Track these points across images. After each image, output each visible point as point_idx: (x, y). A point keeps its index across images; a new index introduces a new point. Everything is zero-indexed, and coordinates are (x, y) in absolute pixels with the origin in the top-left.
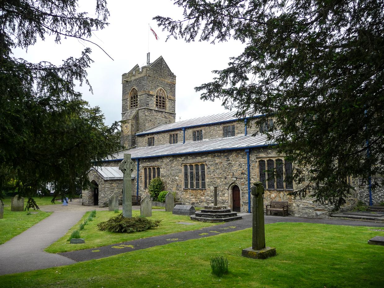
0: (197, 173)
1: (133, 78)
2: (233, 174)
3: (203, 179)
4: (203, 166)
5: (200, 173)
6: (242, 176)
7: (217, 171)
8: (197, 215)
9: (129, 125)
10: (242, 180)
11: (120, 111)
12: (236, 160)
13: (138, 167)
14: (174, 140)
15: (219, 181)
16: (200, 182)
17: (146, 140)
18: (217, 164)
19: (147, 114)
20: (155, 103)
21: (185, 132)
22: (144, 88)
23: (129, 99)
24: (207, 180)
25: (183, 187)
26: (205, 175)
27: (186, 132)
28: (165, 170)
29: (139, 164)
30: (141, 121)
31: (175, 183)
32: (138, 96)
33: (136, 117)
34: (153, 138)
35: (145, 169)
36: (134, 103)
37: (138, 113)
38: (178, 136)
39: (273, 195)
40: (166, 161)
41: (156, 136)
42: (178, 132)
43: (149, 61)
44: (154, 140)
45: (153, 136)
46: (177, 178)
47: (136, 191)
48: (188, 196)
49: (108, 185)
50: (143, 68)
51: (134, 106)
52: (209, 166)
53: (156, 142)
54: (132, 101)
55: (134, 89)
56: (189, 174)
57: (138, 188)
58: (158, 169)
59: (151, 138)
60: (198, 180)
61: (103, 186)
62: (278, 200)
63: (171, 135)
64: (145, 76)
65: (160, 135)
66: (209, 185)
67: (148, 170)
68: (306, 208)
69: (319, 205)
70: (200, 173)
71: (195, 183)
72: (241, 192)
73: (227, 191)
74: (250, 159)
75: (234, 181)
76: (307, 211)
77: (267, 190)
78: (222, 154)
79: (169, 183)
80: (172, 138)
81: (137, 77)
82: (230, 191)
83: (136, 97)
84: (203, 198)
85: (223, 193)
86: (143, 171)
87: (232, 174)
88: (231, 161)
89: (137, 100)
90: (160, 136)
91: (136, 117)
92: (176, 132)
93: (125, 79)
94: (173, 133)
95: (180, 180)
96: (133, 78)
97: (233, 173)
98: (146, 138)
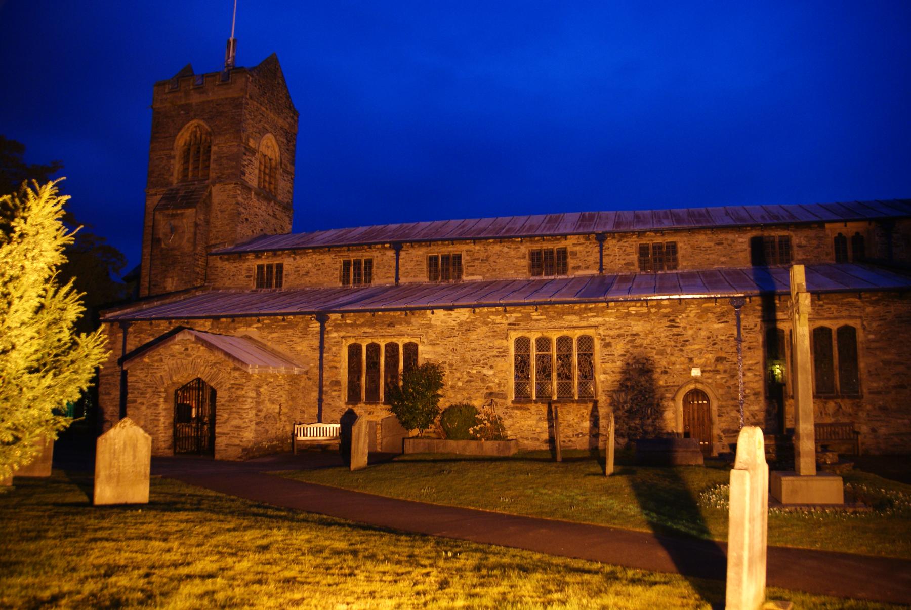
0: (565, 358)
4: (586, 341)
6: (720, 367)
10: (718, 377)
12: (699, 326)
18: (637, 334)
20: (257, 171)
21: (398, 255)
27: (403, 254)
38: (375, 263)
46: (491, 372)
59: (270, 267)
74: (743, 324)
78: (653, 310)
88: (685, 328)
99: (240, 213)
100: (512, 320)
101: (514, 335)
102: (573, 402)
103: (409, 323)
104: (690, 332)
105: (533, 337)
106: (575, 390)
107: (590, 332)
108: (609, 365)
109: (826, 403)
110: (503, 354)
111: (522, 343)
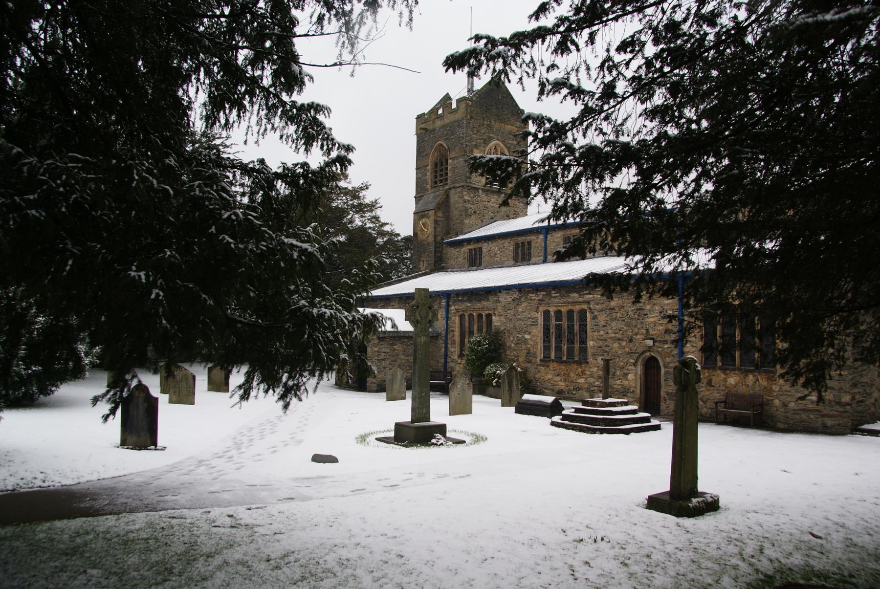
0: (571, 327)
1: (439, 123)
2: (647, 330)
3: (583, 341)
4: (583, 313)
5: (576, 328)
6: (667, 337)
7: (614, 324)
8: (566, 417)
9: (430, 222)
10: (666, 346)
11: (413, 192)
13: (448, 311)
14: (523, 254)
15: (616, 345)
16: (577, 346)
17: (464, 253)
18: (613, 309)
19: (466, 198)
21: (546, 237)
22: (462, 144)
23: (429, 167)
24: (590, 343)
25: (540, 356)
26: (586, 332)
27: (549, 236)
28: (503, 319)
29: (448, 306)
30: (455, 213)
31: (524, 346)
32: (450, 161)
33: (444, 205)
34: (481, 249)
35: (462, 317)
36: (441, 175)
37: (448, 196)
38: (533, 245)
39: (732, 380)
40: (505, 298)
41: (486, 244)
42: (532, 237)
43: (472, 87)
44: (481, 254)
45: (479, 245)
46: (527, 337)
47: (443, 361)
48: (550, 376)
49: (385, 348)
50: (459, 101)
51: (441, 181)
52: (596, 313)
53: (485, 259)
54: (436, 172)
55: (441, 145)
56: (553, 330)
57: (446, 355)
58: (489, 316)
59: (475, 249)
60: (571, 341)
61: (376, 349)
62: (742, 389)
63: (517, 245)
64: (463, 119)
65: (495, 244)
66: (594, 355)
67: (467, 318)
68: (801, 410)
69: (832, 406)
70: (576, 328)
71: (565, 348)
72: (663, 371)
73: (633, 368)
75: (650, 347)
76: (804, 416)
77: (720, 369)
79: (510, 347)
80: (520, 250)
81: (446, 121)
82: (639, 369)
83: (444, 163)
84: (582, 380)
85: (625, 371)
86: (457, 319)
87: (644, 331)
89: (447, 169)
90: (494, 246)
91: (444, 205)
92: (529, 238)
93: (423, 126)
94: (521, 239)
95: (535, 341)
96: (439, 123)
97: (647, 330)
98: (466, 249)
99: (466, 210)
100: (540, 297)
101: (542, 309)
102: (574, 362)
103: (488, 300)
104: (648, 307)
105: (552, 310)
106: (553, 356)
107: (585, 307)
108: (595, 333)
109: (746, 375)
110: (535, 323)
111: (547, 314)
